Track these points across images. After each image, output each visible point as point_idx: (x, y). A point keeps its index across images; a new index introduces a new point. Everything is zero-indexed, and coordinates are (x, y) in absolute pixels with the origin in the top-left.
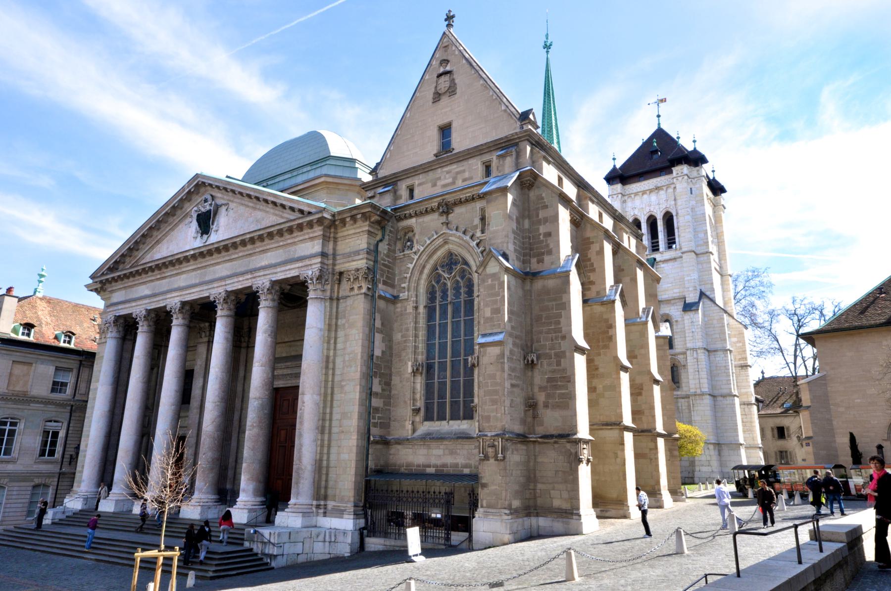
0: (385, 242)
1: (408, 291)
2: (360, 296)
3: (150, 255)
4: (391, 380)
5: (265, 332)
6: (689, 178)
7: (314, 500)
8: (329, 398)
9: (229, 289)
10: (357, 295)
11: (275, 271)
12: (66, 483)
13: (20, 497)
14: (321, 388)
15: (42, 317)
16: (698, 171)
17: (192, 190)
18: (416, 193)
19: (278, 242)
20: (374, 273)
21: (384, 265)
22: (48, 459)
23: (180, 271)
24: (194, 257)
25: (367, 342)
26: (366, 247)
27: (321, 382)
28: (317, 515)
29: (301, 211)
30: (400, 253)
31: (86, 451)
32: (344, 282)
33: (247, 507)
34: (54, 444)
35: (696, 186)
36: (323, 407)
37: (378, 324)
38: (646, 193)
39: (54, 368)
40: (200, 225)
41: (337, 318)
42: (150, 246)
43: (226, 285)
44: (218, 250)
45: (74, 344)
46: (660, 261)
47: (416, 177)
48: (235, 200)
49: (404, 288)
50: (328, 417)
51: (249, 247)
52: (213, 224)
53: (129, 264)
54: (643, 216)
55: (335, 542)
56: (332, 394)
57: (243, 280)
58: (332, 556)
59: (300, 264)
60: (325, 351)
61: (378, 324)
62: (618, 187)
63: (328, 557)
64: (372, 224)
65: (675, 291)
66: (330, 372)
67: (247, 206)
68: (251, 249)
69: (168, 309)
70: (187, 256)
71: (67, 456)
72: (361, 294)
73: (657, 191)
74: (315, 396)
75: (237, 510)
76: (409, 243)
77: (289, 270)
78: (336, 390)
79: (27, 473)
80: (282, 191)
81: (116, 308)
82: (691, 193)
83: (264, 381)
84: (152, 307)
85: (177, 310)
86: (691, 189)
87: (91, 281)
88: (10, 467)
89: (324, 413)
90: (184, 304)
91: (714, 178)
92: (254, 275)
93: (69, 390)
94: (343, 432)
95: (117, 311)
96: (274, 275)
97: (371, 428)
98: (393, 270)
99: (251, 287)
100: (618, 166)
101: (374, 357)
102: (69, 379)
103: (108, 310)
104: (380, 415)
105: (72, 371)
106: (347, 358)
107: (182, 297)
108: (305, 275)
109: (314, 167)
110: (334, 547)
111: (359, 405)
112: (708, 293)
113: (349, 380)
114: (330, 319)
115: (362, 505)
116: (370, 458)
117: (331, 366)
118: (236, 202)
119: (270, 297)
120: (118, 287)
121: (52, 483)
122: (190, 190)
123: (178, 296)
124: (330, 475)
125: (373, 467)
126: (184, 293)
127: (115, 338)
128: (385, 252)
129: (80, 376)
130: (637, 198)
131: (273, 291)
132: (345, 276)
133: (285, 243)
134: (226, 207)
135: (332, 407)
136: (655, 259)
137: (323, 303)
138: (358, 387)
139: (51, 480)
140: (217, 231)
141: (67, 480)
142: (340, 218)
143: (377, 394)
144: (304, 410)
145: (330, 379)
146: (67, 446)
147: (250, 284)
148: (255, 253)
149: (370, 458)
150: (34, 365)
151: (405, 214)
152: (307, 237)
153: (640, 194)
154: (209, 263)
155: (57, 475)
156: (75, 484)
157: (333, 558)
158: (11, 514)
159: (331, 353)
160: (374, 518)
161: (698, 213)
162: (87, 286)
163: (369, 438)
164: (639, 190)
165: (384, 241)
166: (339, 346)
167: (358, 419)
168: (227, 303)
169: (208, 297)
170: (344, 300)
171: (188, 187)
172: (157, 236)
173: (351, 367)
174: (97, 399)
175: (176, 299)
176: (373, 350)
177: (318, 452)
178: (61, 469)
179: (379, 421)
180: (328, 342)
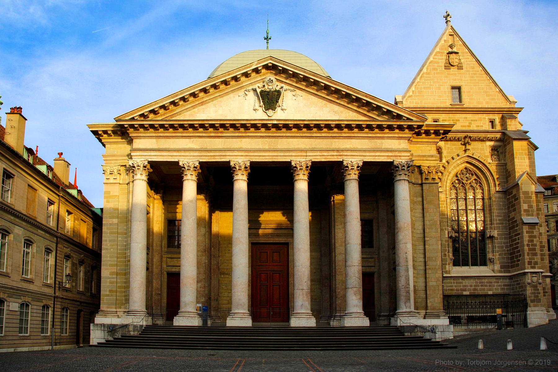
3: (189, 113)
11: (364, 154)
23: (244, 135)
42: (193, 105)
59: (390, 154)
69: (232, 164)
75: (358, 318)
77: (379, 156)
92: (341, 154)
94: (430, 269)
108: (398, 163)
113: (431, 237)
123: (242, 156)
127: (145, 181)
146: (57, 273)
154: (284, 135)
173: (433, 229)
178: (55, 293)
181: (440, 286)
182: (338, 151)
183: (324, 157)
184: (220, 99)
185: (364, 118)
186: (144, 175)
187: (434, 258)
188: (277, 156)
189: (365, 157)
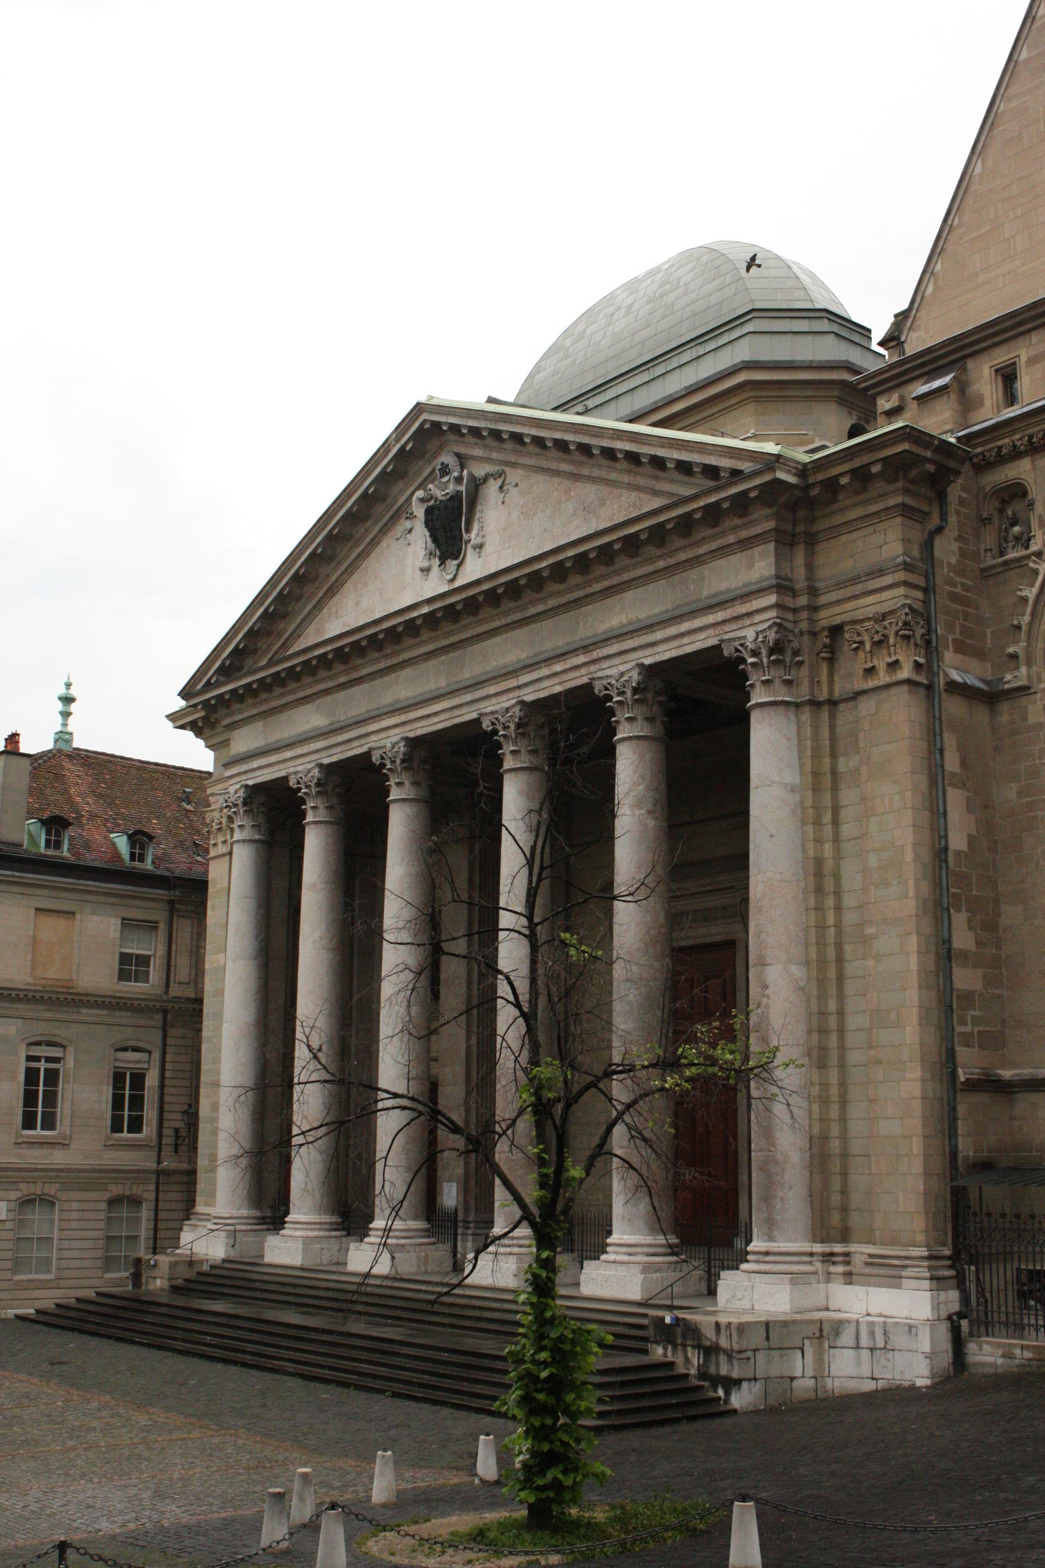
0: (951, 531)
1: (1029, 664)
2: (894, 691)
4: (999, 915)
5: (638, 805)
7: (814, 1241)
8: (832, 973)
9: (529, 698)
10: (888, 686)
11: (649, 638)
12: (175, 1196)
13: (86, 1225)
14: (807, 945)
15: (78, 799)
17: (408, 448)
18: (1025, 384)
19: (652, 560)
20: (928, 621)
21: (954, 597)
22: (127, 1140)
24: (430, 619)
25: (927, 813)
26: (901, 552)
27: (806, 929)
28: (828, 1277)
29: (711, 472)
30: (994, 558)
31: (216, 1120)
32: (845, 650)
33: (638, 1259)
34: (137, 1102)
36: (819, 997)
37: (952, 762)
39: (119, 922)
40: (435, 539)
41: (834, 755)
42: (314, 602)
43: (519, 687)
44: (493, 598)
45: (153, 862)
47: (1021, 342)
48: (523, 460)
49: (1014, 657)
50: (833, 1022)
51: (574, 580)
52: (468, 530)
53: (265, 653)
55: (885, 1348)
56: (840, 960)
57: (565, 671)
58: (881, 1384)
59: (720, 616)
60: (811, 847)
61: (952, 762)
63: (870, 1386)
64: (911, 487)
66: (830, 902)
67: (557, 473)
68: (578, 587)
70: (413, 619)
71: (168, 1132)
72: (899, 683)
74: (794, 969)
76: (1017, 529)
77: (690, 632)
78: (848, 948)
79: (94, 1171)
80: (630, 421)
81: (245, 767)
83: (648, 933)
84: (334, 759)
85: (398, 761)
87: (183, 703)
88: (58, 1158)
89: (823, 1014)
90: (414, 743)
93: (155, 973)
94: (879, 1062)
95: (250, 775)
96: (649, 651)
97: (958, 1048)
98: (977, 609)
99: (588, 687)
101: (951, 854)
102: (152, 947)
103: (228, 773)
104: (977, 1013)
105: (156, 928)
106: (873, 861)
107: (407, 728)
108: (737, 644)
109: (712, 345)
110: (883, 1362)
111: (920, 987)
114: (816, 756)
115: (947, 1252)
116: (961, 1130)
117: (829, 884)
118: (524, 466)
119: (638, 711)
120: (246, 714)
121: (146, 1195)
122: (403, 447)
123: (396, 726)
124: (852, 1177)
125: (971, 1153)
126: (412, 715)
128: (953, 560)
129: (174, 941)
131: (649, 696)
132: (847, 636)
133: (671, 561)
134: (499, 482)
135: (841, 996)
137: (793, 718)
138: (914, 939)
139: (142, 1187)
140: (481, 546)
141: (174, 1187)
142: (821, 477)
143: (964, 955)
144: (767, 1007)
145: (831, 920)
146: (167, 1107)
147: (585, 680)
148: (592, 594)
149: (961, 1127)
150: (78, 916)
151: (1000, 448)
152: (731, 539)
155: (153, 1177)
156: (199, 1199)
157: (885, 1391)
158: (74, 1264)
159: (828, 850)
160: (987, 1286)
162: (172, 717)
163: (953, 1074)
165: (946, 531)
166: (847, 830)
167: (921, 1025)
168: (523, 735)
169: (477, 722)
170: (850, 704)
171: (397, 440)
172: (328, 576)
174: (226, 992)
175: (392, 732)
176: (946, 837)
177: (816, 1115)
178: (159, 1162)
179: (976, 1029)
180: (817, 822)
181: (914, 1138)
182: (585, 648)
183: (557, 680)
184: (366, 564)
185: (657, 503)
186: (248, 828)
187: (893, 1016)
188: (460, 706)
189: (656, 649)
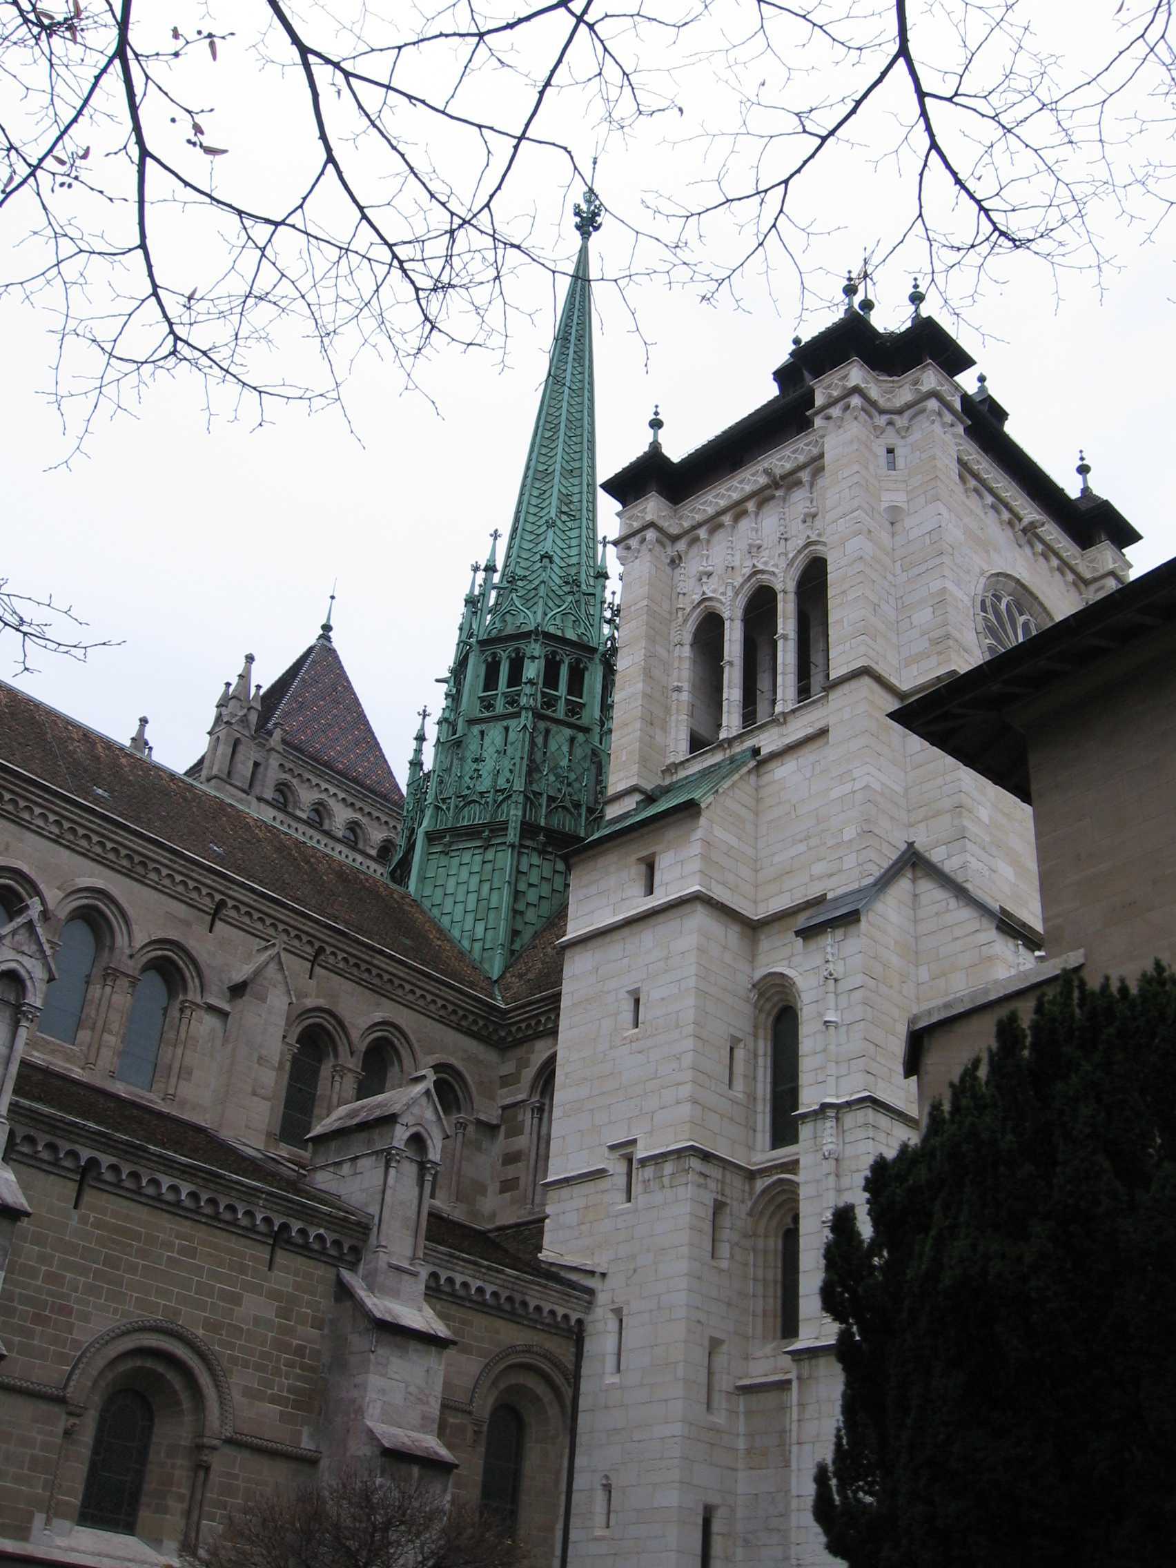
6: (882, 412)
16: (916, 383)
35: (910, 439)
38: (745, 513)
46: (774, 756)
54: (730, 593)
62: (652, 507)
65: (819, 868)
73: (778, 493)
82: (892, 465)
86: (890, 451)
91: (1086, 490)
100: (677, 450)
112: (936, 856)
130: (720, 536)
136: (756, 751)
153: (727, 519)
161: (913, 534)
164: (723, 503)
